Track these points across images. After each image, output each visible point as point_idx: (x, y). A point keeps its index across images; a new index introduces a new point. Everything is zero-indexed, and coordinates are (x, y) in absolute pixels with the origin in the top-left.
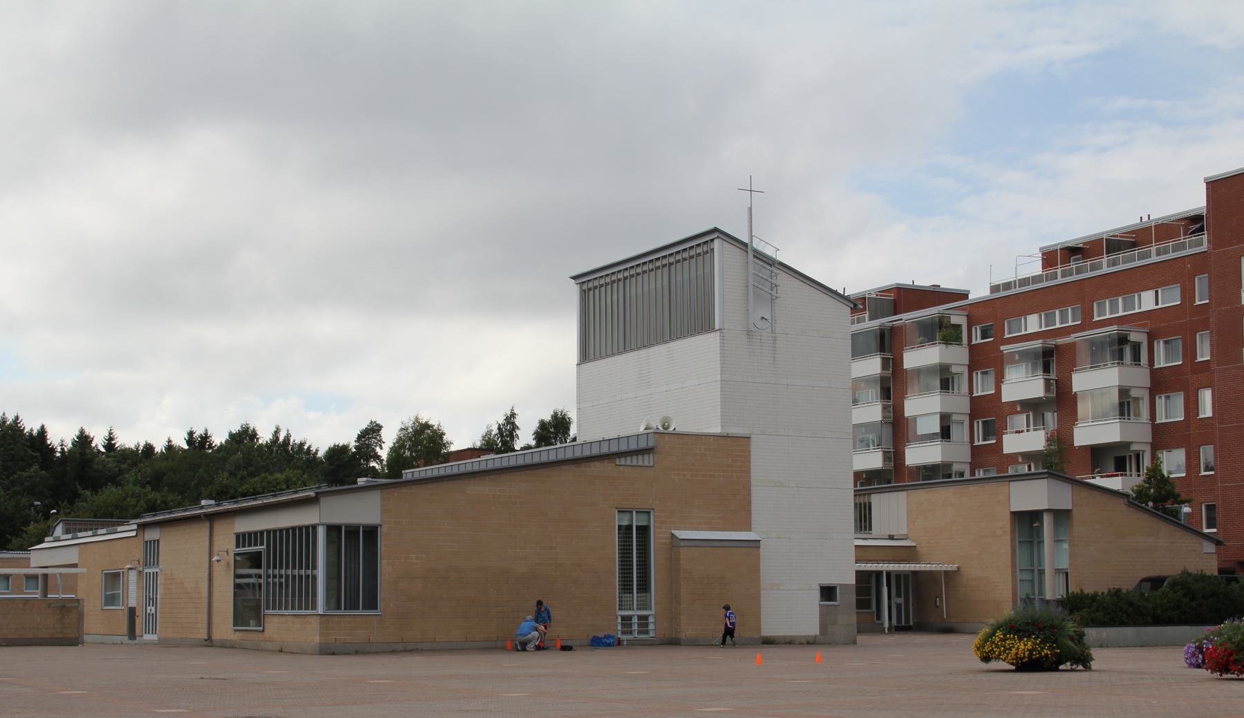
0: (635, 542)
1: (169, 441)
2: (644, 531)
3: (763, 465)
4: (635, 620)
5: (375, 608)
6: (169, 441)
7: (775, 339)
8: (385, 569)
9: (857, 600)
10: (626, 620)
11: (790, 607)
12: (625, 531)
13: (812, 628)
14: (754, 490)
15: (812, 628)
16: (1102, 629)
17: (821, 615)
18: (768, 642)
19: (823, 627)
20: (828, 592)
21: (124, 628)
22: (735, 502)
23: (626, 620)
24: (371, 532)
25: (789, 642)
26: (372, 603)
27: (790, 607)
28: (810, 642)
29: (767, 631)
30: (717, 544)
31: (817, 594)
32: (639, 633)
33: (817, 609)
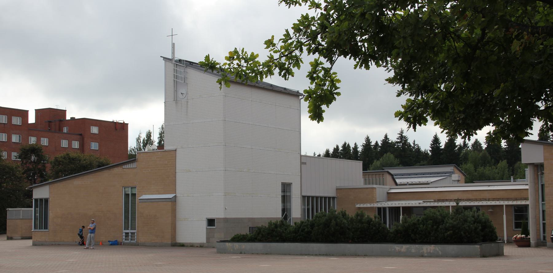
0: (130, 199)
1: (386, 136)
2: (134, 195)
3: (182, 163)
4: (130, 234)
5: (47, 229)
6: (386, 136)
7: (187, 102)
8: (51, 215)
9: (515, 215)
10: (127, 234)
11: (192, 230)
12: (127, 195)
13: (202, 239)
14: (178, 175)
15: (202, 239)
16: (240, 244)
17: (207, 233)
18: (182, 245)
19: (208, 239)
20: (211, 222)
21: (546, 213)
22: (169, 181)
23: (127, 234)
24: (46, 200)
25: (192, 246)
26: (46, 227)
27: (192, 230)
28: (201, 246)
29: (181, 239)
30: (149, 201)
31: (205, 223)
32: (126, 240)
33: (205, 230)
